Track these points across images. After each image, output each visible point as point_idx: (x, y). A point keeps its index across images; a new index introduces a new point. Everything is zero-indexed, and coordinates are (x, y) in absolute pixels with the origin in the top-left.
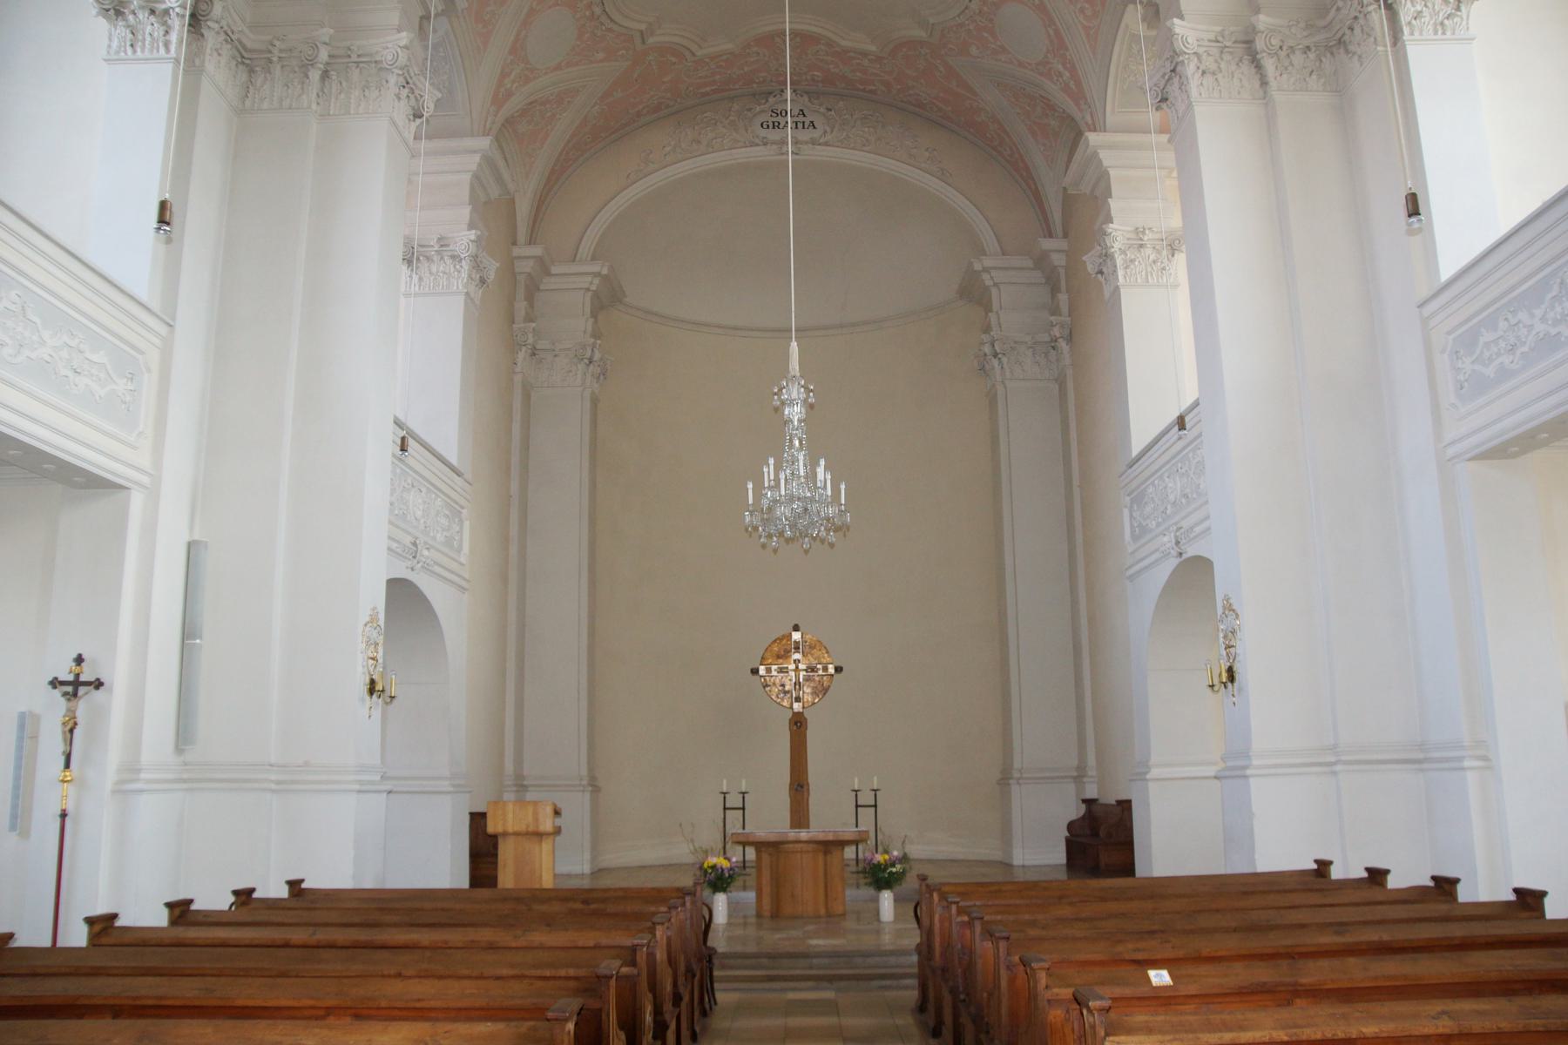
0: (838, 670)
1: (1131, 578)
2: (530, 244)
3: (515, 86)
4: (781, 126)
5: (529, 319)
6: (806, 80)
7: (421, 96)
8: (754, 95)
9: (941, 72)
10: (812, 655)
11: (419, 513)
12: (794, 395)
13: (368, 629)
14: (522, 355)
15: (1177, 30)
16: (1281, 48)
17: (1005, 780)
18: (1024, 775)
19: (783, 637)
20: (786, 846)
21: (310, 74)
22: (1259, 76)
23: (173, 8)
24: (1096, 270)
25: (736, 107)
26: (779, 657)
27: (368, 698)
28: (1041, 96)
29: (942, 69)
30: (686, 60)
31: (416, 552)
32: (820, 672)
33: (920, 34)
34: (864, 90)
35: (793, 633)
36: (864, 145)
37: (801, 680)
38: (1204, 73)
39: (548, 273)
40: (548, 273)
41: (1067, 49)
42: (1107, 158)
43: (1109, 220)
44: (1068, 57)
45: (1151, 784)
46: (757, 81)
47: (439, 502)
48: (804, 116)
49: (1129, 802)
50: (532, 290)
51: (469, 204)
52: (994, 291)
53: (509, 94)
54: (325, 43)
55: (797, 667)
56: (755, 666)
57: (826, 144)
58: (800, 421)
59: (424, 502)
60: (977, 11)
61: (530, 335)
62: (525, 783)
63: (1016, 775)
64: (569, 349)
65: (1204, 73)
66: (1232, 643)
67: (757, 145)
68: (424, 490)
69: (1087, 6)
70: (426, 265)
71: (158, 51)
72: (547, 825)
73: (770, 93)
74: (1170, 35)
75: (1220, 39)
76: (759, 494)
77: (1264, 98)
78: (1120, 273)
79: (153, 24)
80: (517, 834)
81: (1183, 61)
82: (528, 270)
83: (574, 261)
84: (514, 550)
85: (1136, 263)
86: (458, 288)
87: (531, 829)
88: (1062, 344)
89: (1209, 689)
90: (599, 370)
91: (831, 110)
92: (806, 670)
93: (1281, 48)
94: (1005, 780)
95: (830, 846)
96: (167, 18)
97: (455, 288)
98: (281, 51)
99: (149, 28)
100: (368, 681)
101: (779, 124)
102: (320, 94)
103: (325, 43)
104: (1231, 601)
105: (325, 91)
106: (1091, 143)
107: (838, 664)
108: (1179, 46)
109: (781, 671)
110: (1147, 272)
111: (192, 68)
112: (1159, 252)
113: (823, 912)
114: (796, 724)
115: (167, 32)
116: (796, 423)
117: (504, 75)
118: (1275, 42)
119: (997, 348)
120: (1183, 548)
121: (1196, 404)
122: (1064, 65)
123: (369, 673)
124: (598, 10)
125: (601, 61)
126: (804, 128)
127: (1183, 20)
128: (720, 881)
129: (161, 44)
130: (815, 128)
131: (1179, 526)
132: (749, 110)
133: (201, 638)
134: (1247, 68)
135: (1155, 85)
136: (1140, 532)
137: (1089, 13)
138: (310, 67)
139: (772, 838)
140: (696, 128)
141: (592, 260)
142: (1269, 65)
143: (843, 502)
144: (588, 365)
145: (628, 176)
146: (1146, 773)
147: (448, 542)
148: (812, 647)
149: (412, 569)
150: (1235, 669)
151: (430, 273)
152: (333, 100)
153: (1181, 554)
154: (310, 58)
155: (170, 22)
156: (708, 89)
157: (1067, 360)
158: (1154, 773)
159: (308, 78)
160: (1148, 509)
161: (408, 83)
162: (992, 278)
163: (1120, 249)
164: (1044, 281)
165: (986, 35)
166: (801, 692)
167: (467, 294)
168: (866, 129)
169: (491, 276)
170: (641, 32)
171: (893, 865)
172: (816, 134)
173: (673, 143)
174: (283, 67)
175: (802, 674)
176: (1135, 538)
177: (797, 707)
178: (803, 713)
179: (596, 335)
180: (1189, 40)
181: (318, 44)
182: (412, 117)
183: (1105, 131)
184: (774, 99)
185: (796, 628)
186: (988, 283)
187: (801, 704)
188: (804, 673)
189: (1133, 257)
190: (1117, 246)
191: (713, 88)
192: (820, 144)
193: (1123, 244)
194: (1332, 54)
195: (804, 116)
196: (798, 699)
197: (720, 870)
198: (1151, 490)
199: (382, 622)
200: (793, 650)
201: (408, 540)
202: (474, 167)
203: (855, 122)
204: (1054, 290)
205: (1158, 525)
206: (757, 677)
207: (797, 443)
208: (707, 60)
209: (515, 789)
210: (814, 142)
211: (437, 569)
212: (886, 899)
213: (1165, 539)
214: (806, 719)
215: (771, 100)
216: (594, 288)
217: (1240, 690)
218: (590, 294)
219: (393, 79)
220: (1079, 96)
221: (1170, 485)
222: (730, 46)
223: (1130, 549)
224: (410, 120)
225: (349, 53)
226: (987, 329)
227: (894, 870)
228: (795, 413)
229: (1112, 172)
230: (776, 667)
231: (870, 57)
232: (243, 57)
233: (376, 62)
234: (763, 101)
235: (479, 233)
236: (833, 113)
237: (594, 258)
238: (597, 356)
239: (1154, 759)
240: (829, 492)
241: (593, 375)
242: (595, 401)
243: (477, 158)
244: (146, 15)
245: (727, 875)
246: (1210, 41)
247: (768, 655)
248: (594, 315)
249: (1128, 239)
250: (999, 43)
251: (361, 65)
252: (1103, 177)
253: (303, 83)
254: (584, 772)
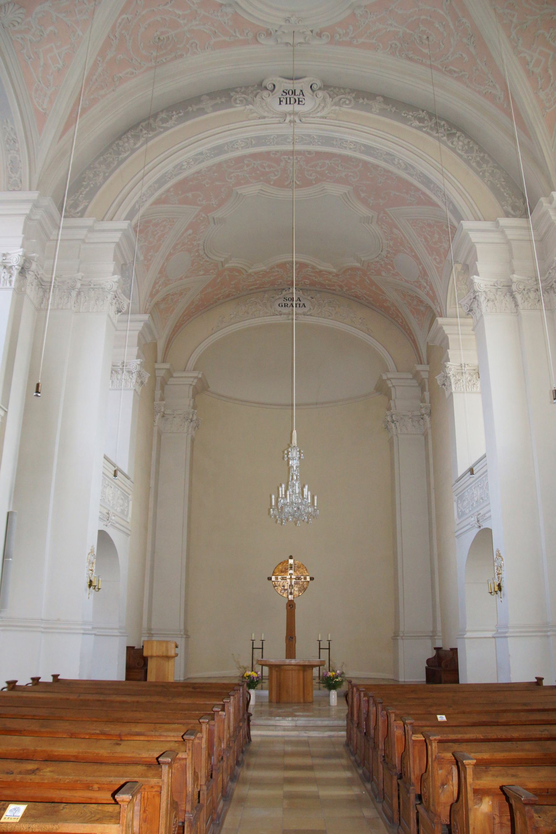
0: (312, 579)
1: (457, 537)
2: (163, 362)
3: (161, 287)
4: (288, 306)
5: (162, 399)
6: (302, 284)
7: (121, 303)
8: (275, 290)
9: (367, 282)
10: (299, 571)
11: (110, 498)
12: (294, 455)
13: (90, 556)
14: (158, 417)
15: (476, 281)
16: (524, 289)
17: (395, 637)
18: (405, 635)
19: (285, 561)
20: (285, 667)
21: (72, 293)
22: (514, 302)
23: (14, 266)
24: (442, 384)
25: (266, 296)
26: (282, 572)
27: (88, 589)
28: (416, 296)
29: (368, 281)
30: (243, 274)
31: (109, 517)
32: (303, 580)
33: (358, 265)
34: (330, 289)
35: (289, 560)
36: (329, 316)
37: (293, 584)
38: (488, 300)
39: (172, 376)
40: (172, 376)
41: (428, 276)
42: (447, 330)
43: (448, 360)
44: (429, 280)
45: (467, 641)
46: (277, 284)
47: (119, 492)
48: (300, 301)
49: (457, 649)
50: (164, 383)
51: (137, 346)
52: (393, 389)
53: (158, 292)
54: (80, 280)
55: (291, 577)
56: (270, 576)
57: (311, 315)
58: (297, 467)
59: (113, 493)
60: (385, 256)
61: (162, 408)
62: (152, 632)
63: (401, 635)
64: (181, 414)
65: (488, 300)
66: (500, 572)
67: (277, 315)
68: (113, 487)
69: (437, 257)
70: (116, 375)
71: (6, 285)
72: (172, 653)
73: (284, 289)
74: (472, 282)
75: (496, 285)
76: (277, 502)
77: (517, 313)
78: (453, 386)
79: (5, 273)
80: (158, 657)
81: (478, 295)
82: (162, 375)
83: (184, 371)
84: (151, 514)
85: (461, 381)
86: (130, 387)
87: (164, 654)
88: (426, 417)
89: (489, 594)
90: (195, 425)
91: (313, 298)
92: (295, 579)
93: (524, 289)
94: (395, 637)
95: (306, 668)
96: (11, 270)
97: (129, 387)
98: (59, 282)
99: (3, 275)
100: (89, 580)
101: (288, 304)
102: (76, 302)
103: (80, 280)
104: (500, 552)
105: (78, 300)
106: (439, 323)
107: (312, 576)
108: (476, 288)
109: (283, 579)
110: (466, 385)
111: (19, 292)
112: (472, 376)
113: (302, 700)
114: (290, 606)
115: (11, 276)
116: (295, 468)
117: (155, 283)
118: (521, 287)
119: (394, 418)
120: (481, 523)
121: (485, 456)
122: (427, 283)
123: (89, 576)
124: (201, 253)
125: (202, 275)
126: (300, 307)
127: (479, 276)
128: (252, 683)
129: (8, 282)
130: (305, 307)
131: (479, 513)
132: (273, 297)
133: (12, 558)
134: (508, 298)
135: (467, 304)
136: (462, 514)
137: (438, 260)
138: (72, 290)
139: (278, 663)
140: (247, 306)
141: (193, 370)
142: (519, 297)
143: (316, 505)
144: (190, 422)
145: (212, 329)
146: (465, 635)
147: (122, 512)
148: (299, 567)
149: (106, 526)
150: (501, 585)
151: (117, 379)
152: (81, 305)
153: (480, 527)
154: (72, 286)
155: (12, 272)
156: (253, 287)
157: (428, 425)
158: (468, 635)
159: (71, 295)
160: (465, 503)
161: (116, 297)
162: (392, 383)
163: (453, 374)
164: (417, 385)
165: (389, 267)
166: (293, 590)
167: (135, 390)
168: (330, 308)
169: (146, 381)
170: (222, 262)
171: (337, 678)
172: (305, 310)
173: (235, 313)
174: (59, 289)
175: (293, 581)
176: (459, 517)
177: (291, 597)
178: (293, 600)
179: (194, 407)
180: (482, 286)
181: (76, 280)
182: (116, 313)
183: (446, 317)
184: (286, 292)
185: (291, 557)
186: (390, 385)
187: (293, 596)
188: (295, 580)
189: (459, 378)
190: (451, 373)
191: (255, 287)
192: (307, 315)
193: (455, 372)
194: (548, 292)
195: (300, 301)
196: (291, 593)
197: (252, 678)
198: (466, 494)
199: (95, 553)
200: (289, 569)
201: (105, 511)
202: (140, 328)
203: (325, 304)
204: (423, 390)
205: (470, 511)
206: (270, 582)
207: (295, 478)
208: (253, 274)
209: (147, 635)
210: (304, 314)
211: (117, 525)
212: (334, 694)
213: (472, 519)
214: (295, 604)
215: (284, 293)
216: (194, 384)
217: (504, 594)
218: (192, 387)
219: (110, 297)
220: (434, 298)
221: (475, 492)
222: (264, 268)
223: (457, 522)
224: (116, 314)
225: (90, 283)
226: (389, 409)
227: (337, 680)
228: (294, 463)
229: (449, 336)
230: (280, 577)
231: (333, 274)
232: (41, 285)
233: (102, 288)
234: (280, 293)
235: (142, 360)
236: (314, 299)
237: (194, 370)
238: (195, 418)
239: (468, 628)
240: (309, 501)
241: (192, 427)
242: (193, 440)
243: (142, 324)
244: (2, 268)
245: (256, 681)
246: (491, 285)
247: (276, 570)
248: (194, 397)
249: (457, 369)
250: (396, 271)
251: (95, 289)
252: (445, 339)
253: (68, 297)
254: (182, 627)
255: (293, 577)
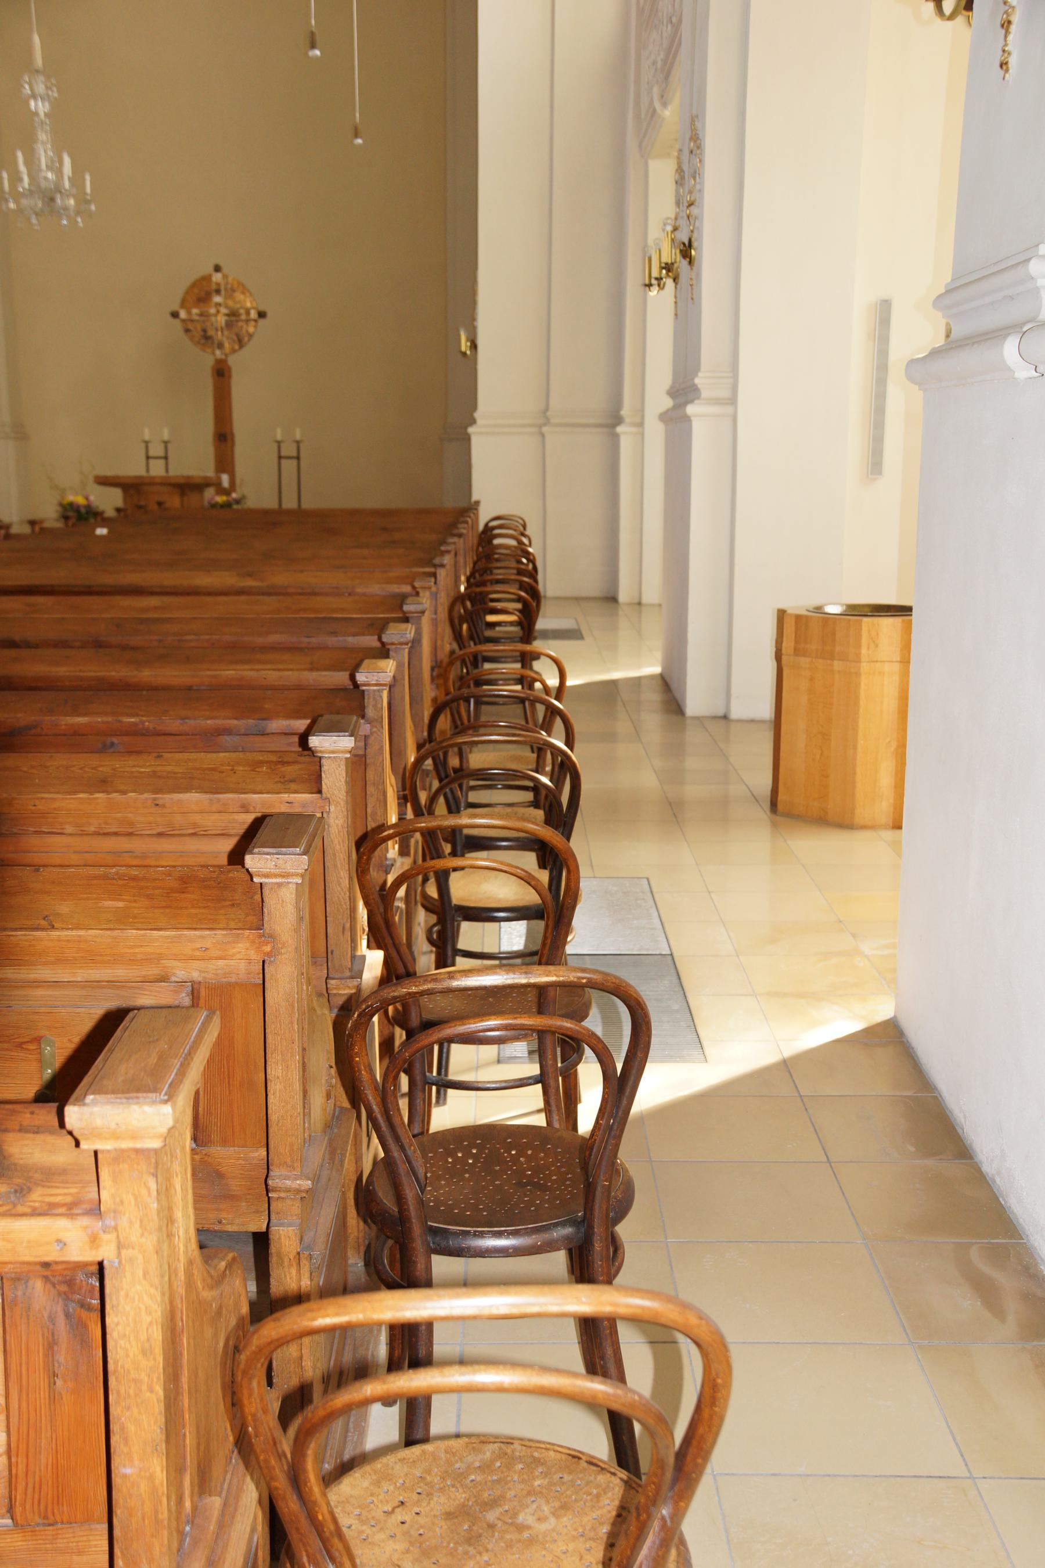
55: (218, 312)
58: (46, 115)
107: (261, 308)
185: (217, 269)
214: (229, 369)
228: (40, 107)
255: (223, 310)
